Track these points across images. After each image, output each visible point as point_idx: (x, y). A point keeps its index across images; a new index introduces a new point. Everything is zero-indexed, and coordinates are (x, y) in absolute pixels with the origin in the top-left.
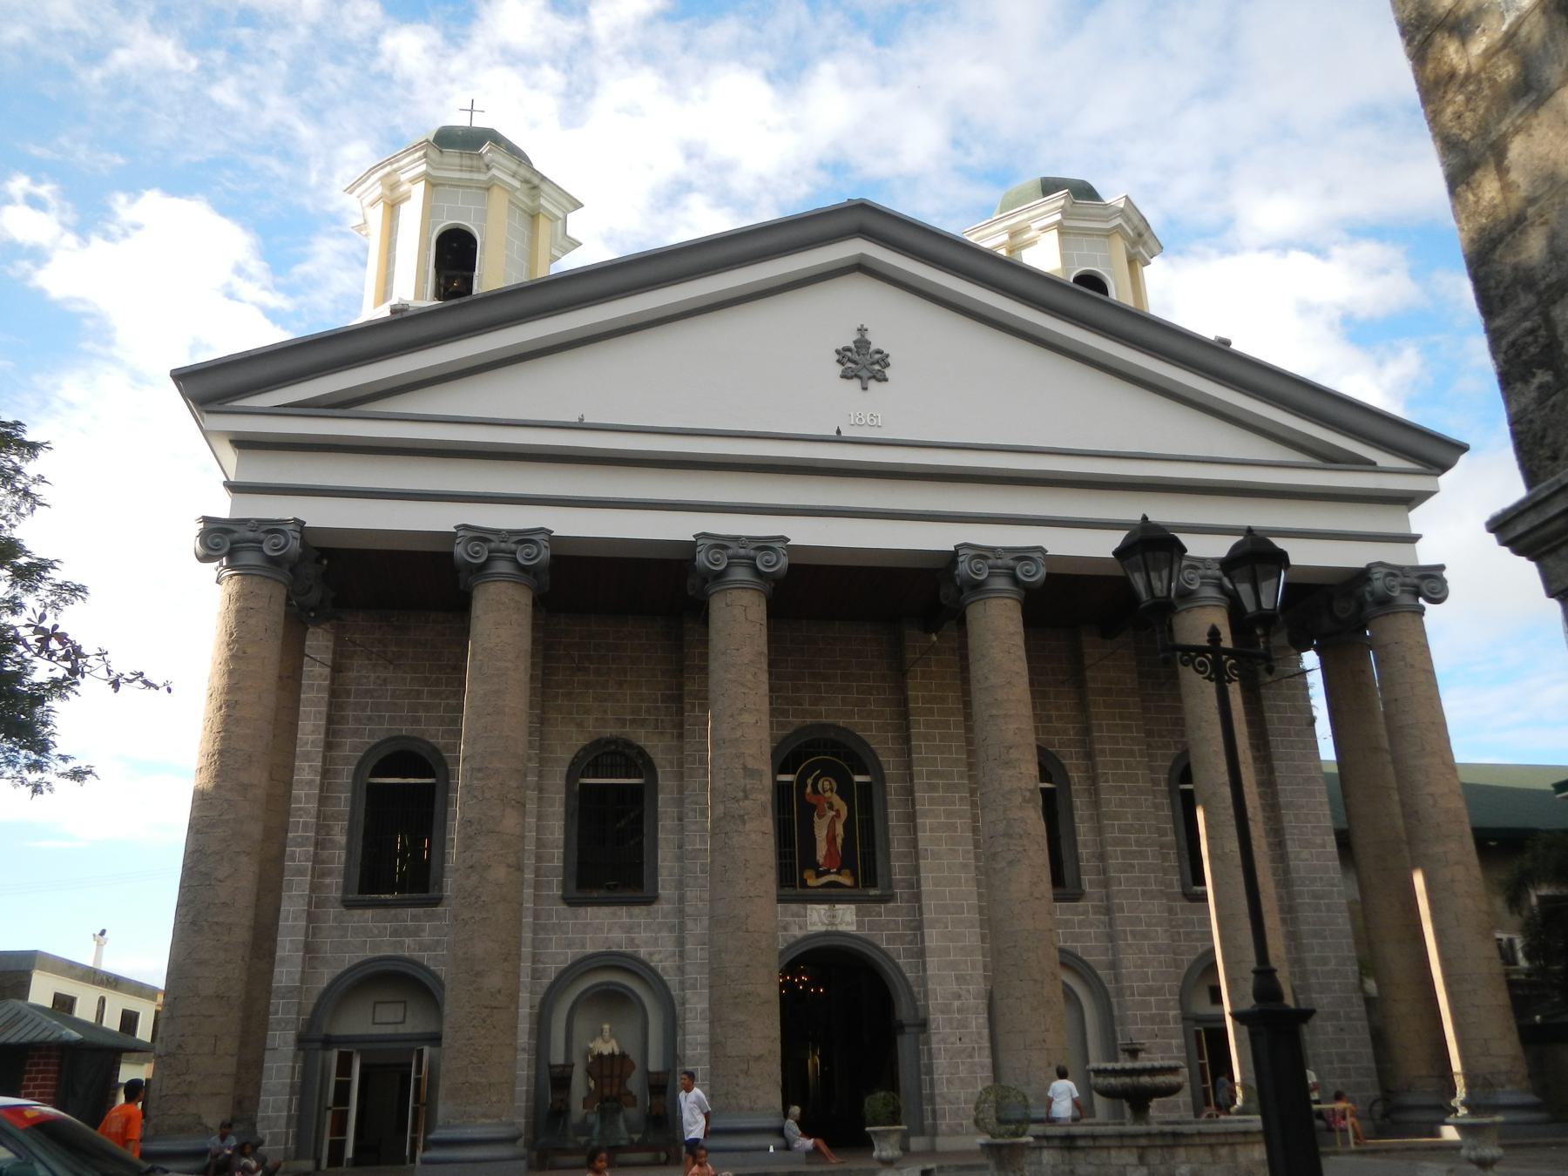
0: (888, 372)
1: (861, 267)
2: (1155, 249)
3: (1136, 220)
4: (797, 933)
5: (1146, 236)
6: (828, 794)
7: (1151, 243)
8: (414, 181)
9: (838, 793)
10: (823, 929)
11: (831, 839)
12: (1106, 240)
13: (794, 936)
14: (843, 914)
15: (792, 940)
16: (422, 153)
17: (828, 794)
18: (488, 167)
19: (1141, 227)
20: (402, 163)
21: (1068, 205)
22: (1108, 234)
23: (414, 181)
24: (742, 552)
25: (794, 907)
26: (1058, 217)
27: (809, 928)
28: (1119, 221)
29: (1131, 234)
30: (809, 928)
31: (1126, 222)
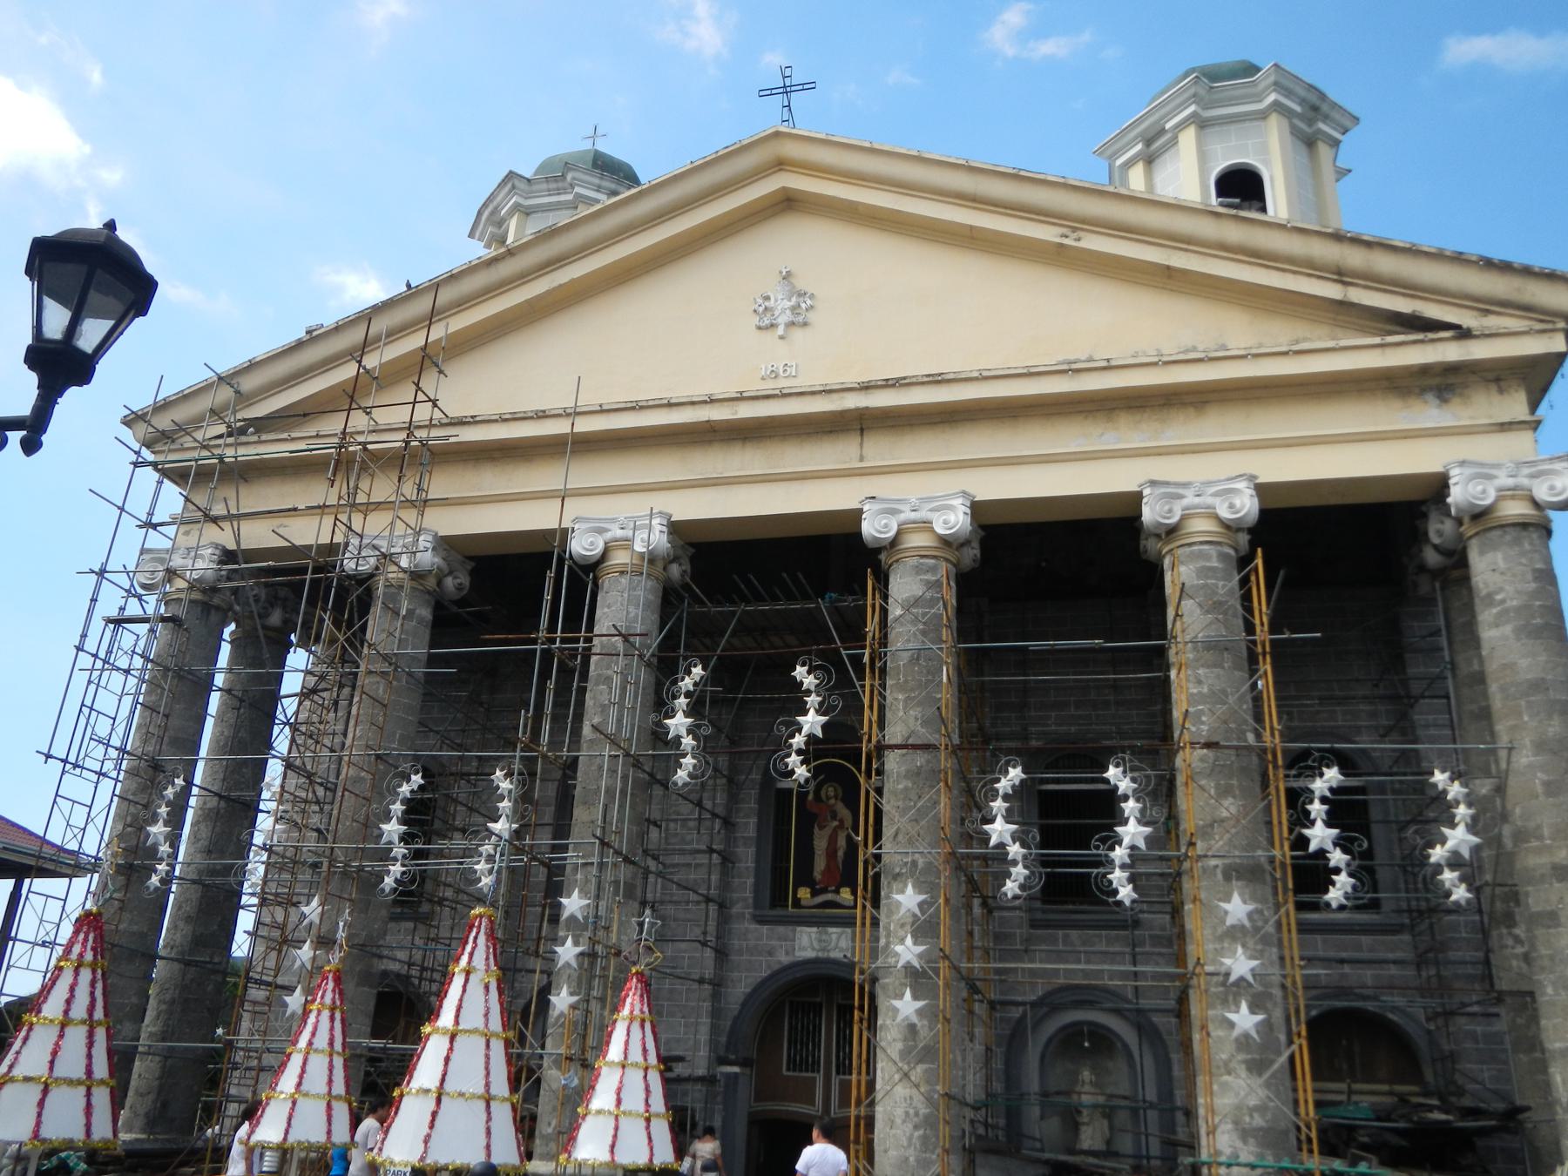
0: (811, 316)
1: (788, 203)
2: (1347, 123)
3: (1301, 92)
4: (785, 959)
5: (1325, 108)
6: (832, 801)
7: (1336, 115)
8: (511, 213)
9: (843, 800)
10: (810, 954)
11: (831, 853)
12: (1261, 123)
13: (780, 962)
14: (838, 939)
15: (776, 967)
16: (509, 185)
17: (832, 801)
18: (572, 186)
19: (1313, 98)
20: (499, 199)
21: (1202, 92)
22: (1263, 115)
23: (511, 213)
24: (619, 533)
25: (781, 929)
26: (1192, 108)
27: (797, 954)
28: (1272, 97)
29: (1298, 109)
30: (797, 954)
31: (1286, 97)
